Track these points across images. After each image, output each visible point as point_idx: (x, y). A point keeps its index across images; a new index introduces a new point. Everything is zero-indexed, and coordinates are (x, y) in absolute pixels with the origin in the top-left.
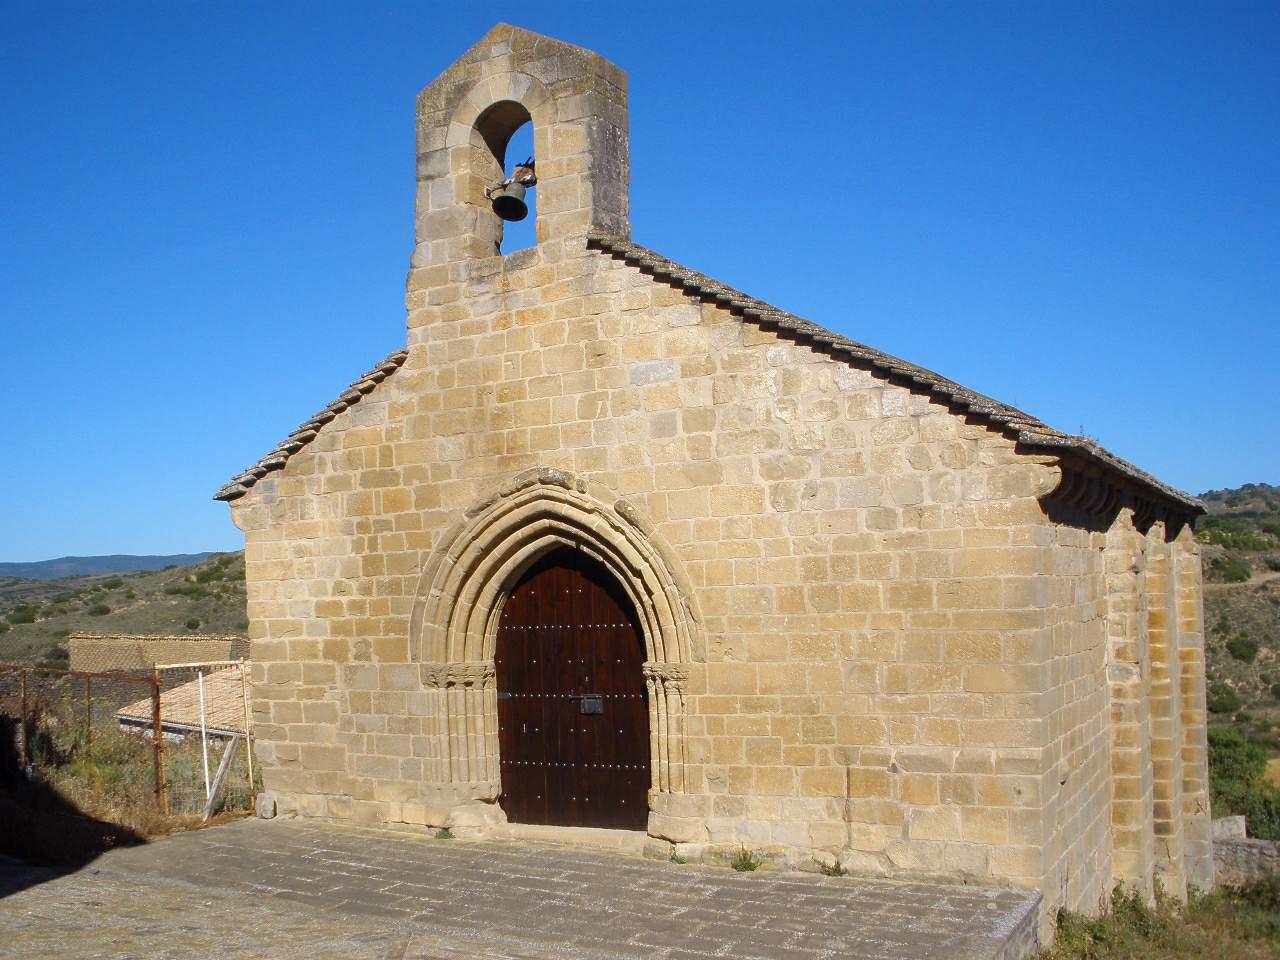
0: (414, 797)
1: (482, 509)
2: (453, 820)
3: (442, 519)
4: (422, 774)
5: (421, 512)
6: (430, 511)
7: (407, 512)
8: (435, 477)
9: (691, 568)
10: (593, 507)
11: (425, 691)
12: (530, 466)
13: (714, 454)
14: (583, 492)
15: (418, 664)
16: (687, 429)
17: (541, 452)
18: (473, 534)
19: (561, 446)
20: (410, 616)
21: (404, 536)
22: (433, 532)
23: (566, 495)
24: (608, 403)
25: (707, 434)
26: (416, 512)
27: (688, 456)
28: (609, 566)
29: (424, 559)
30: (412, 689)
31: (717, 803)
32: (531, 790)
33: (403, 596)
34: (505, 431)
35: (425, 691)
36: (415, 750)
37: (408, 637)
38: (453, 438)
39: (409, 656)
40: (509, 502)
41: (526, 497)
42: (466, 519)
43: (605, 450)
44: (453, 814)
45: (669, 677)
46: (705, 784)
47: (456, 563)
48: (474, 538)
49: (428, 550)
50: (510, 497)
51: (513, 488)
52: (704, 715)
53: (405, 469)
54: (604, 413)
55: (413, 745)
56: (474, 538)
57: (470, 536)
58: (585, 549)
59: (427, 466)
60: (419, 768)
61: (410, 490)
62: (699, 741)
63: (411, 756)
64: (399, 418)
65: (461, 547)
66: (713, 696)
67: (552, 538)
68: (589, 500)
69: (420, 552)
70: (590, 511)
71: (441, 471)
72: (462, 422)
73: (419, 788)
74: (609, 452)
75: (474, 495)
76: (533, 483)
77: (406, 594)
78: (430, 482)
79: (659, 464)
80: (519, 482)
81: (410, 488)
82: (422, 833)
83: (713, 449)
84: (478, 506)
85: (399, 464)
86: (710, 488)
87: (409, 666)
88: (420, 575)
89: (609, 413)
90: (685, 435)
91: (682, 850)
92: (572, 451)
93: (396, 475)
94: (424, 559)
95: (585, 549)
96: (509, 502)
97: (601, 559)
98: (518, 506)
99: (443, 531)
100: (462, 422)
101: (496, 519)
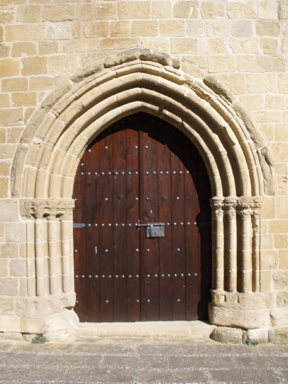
0: (10, 310)
1: (87, 76)
2: (48, 326)
3: (48, 83)
4: (19, 289)
5: (28, 77)
6: (37, 76)
7: (14, 77)
8: (42, 51)
9: (264, 128)
10: (184, 79)
11: (24, 222)
12: (129, 46)
13: (279, 52)
14: (178, 68)
15: (18, 199)
16: (259, 32)
17: (141, 37)
18: (77, 95)
19: (159, 34)
20: (12, 159)
21: (10, 96)
22: (38, 92)
23: (161, 69)
24: (199, 9)
25: (275, 38)
26: (23, 77)
27: (261, 51)
28: (187, 125)
29: (28, 115)
30: (10, 220)
31: (278, 297)
32: (109, 284)
33: (6, 144)
34: (110, 21)
35: (24, 222)
36: (11, 271)
37: (9, 177)
38: (61, 24)
39: (9, 193)
40: (111, 72)
41: (127, 69)
42: (72, 83)
43: (196, 41)
44: (48, 322)
45: (249, 206)
46: (272, 284)
47: (57, 117)
48: (77, 99)
49: (32, 107)
50: (113, 68)
51: (118, 61)
52: (272, 234)
53: (14, 45)
54: (194, 15)
55: (10, 266)
56: (77, 99)
57: (73, 96)
58: (167, 113)
59: (36, 43)
60: (16, 285)
61: (19, 61)
62: (268, 252)
63: (9, 276)
64: (10, 6)
65: (64, 105)
66: (279, 219)
67: (138, 104)
68: (181, 75)
69: (25, 108)
70: (180, 83)
71: (49, 46)
72: (70, 12)
73: (15, 302)
74: (199, 42)
75: (79, 66)
76: (135, 59)
77: (9, 141)
78: (38, 55)
79: (239, 54)
80: (123, 58)
81: (19, 59)
82: (17, 339)
83: (279, 48)
84: (84, 73)
85: (8, 40)
86: (277, 74)
87: (8, 202)
88: (25, 127)
89: (199, 16)
90: (258, 37)
91: (254, 335)
92: (168, 39)
93: (6, 48)
94: (28, 115)
95: (167, 113)
96: (111, 72)
97: (180, 120)
98: (118, 76)
99: (47, 92)
100: (70, 12)
101: (98, 84)
